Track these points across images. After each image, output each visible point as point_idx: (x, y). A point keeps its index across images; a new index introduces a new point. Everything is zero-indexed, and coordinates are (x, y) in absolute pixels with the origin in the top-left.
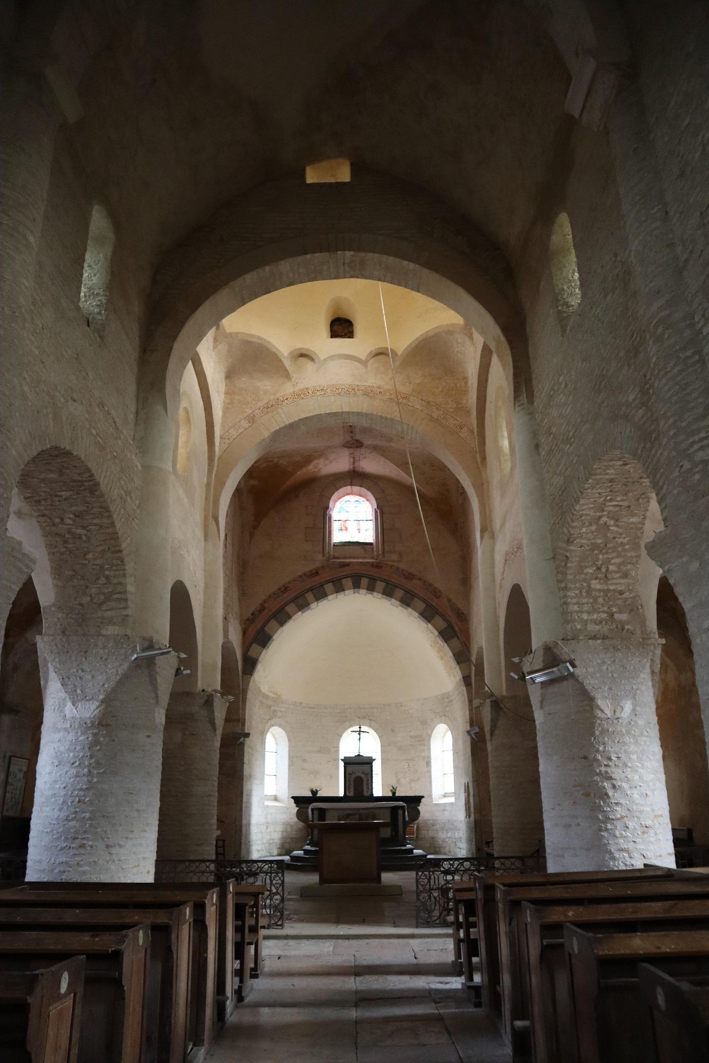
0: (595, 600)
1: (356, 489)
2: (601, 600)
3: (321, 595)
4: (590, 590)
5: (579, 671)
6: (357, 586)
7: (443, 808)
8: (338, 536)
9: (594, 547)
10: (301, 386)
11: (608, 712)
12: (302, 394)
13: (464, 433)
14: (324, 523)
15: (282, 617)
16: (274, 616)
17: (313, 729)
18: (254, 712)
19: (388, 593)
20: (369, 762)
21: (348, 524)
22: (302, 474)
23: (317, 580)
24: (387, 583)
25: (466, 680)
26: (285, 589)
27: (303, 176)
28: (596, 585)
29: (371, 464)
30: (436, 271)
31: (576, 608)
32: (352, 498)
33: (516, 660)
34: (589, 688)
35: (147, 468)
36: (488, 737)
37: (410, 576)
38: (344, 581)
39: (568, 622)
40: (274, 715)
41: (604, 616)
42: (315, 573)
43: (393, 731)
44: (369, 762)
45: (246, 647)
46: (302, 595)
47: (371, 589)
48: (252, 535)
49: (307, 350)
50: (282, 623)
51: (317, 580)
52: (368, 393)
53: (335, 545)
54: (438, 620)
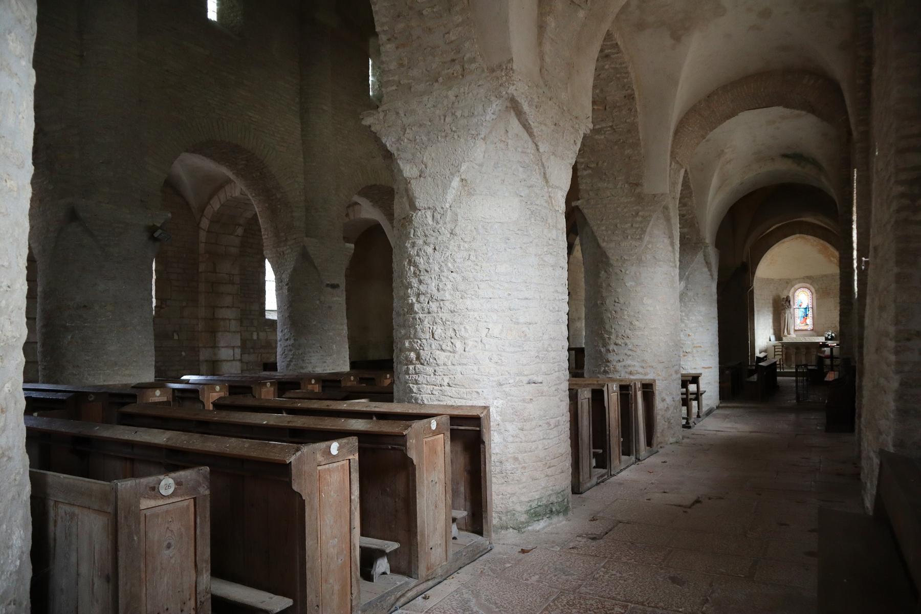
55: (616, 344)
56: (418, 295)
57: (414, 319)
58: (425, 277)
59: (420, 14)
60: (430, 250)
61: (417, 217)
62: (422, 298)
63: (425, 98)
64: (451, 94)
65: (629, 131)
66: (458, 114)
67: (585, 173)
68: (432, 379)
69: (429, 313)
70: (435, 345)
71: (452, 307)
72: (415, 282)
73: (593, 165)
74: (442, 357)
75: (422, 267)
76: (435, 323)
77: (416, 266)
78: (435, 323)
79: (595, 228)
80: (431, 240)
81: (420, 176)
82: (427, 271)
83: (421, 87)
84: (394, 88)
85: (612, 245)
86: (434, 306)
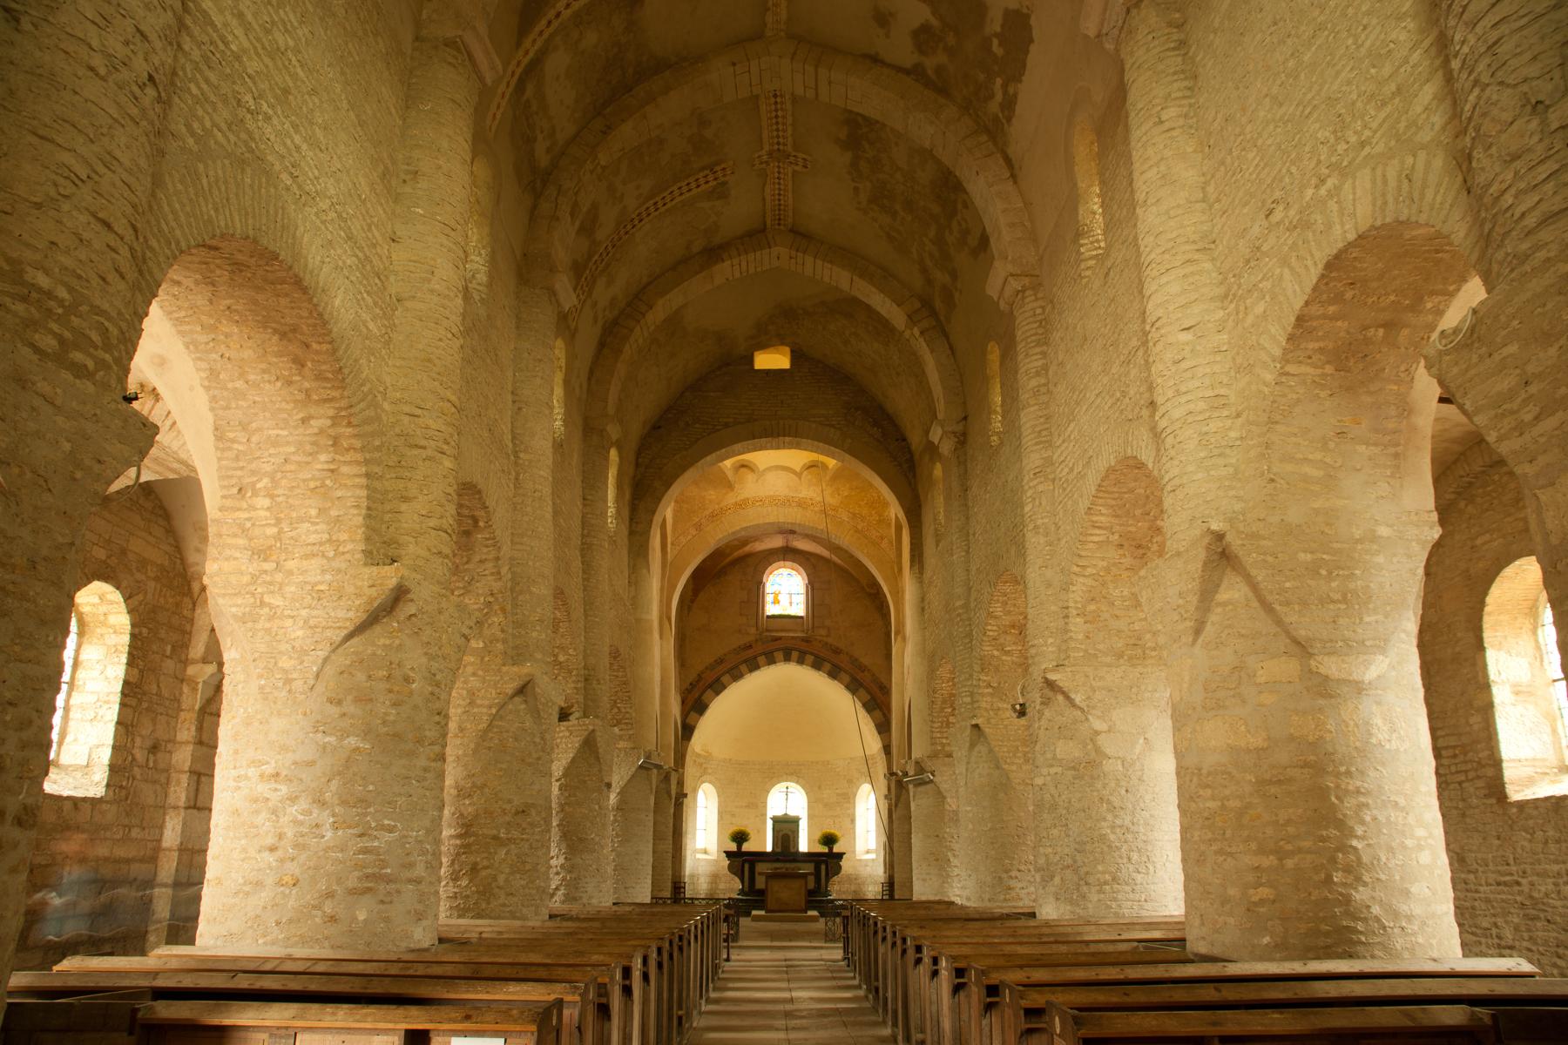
3: (754, 667)
5: (937, 779)
6: (787, 659)
7: (866, 863)
10: (742, 497)
13: (884, 544)
15: (718, 687)
16: (710, 686)
17: (746, 784)
18: (690, 770)
19: (817, 666)
20: (795, 821)
22: (736, 554)
23: (750, 653)
24: (816, 656)
25: (887, 749)
26: (720, 661)
27: (751, 361)
32: (781, 571)
35: (638, 621)
37: (837, 651)
40: (705, 772)
44: (795, 821)
45: (685, 715)
46: (736, 667)
47: (801, 662)
48: (689, 608)
50: (718, 693)
51: (750, 653)
52: (802, 504)
54: (862, 691)
56: (1113, 827)
57: (1110, 847)
61: (1108, 766)
70: (1131, 868)
72: (1110, 817)
74: (1139, 878)
83: (1108, 659)
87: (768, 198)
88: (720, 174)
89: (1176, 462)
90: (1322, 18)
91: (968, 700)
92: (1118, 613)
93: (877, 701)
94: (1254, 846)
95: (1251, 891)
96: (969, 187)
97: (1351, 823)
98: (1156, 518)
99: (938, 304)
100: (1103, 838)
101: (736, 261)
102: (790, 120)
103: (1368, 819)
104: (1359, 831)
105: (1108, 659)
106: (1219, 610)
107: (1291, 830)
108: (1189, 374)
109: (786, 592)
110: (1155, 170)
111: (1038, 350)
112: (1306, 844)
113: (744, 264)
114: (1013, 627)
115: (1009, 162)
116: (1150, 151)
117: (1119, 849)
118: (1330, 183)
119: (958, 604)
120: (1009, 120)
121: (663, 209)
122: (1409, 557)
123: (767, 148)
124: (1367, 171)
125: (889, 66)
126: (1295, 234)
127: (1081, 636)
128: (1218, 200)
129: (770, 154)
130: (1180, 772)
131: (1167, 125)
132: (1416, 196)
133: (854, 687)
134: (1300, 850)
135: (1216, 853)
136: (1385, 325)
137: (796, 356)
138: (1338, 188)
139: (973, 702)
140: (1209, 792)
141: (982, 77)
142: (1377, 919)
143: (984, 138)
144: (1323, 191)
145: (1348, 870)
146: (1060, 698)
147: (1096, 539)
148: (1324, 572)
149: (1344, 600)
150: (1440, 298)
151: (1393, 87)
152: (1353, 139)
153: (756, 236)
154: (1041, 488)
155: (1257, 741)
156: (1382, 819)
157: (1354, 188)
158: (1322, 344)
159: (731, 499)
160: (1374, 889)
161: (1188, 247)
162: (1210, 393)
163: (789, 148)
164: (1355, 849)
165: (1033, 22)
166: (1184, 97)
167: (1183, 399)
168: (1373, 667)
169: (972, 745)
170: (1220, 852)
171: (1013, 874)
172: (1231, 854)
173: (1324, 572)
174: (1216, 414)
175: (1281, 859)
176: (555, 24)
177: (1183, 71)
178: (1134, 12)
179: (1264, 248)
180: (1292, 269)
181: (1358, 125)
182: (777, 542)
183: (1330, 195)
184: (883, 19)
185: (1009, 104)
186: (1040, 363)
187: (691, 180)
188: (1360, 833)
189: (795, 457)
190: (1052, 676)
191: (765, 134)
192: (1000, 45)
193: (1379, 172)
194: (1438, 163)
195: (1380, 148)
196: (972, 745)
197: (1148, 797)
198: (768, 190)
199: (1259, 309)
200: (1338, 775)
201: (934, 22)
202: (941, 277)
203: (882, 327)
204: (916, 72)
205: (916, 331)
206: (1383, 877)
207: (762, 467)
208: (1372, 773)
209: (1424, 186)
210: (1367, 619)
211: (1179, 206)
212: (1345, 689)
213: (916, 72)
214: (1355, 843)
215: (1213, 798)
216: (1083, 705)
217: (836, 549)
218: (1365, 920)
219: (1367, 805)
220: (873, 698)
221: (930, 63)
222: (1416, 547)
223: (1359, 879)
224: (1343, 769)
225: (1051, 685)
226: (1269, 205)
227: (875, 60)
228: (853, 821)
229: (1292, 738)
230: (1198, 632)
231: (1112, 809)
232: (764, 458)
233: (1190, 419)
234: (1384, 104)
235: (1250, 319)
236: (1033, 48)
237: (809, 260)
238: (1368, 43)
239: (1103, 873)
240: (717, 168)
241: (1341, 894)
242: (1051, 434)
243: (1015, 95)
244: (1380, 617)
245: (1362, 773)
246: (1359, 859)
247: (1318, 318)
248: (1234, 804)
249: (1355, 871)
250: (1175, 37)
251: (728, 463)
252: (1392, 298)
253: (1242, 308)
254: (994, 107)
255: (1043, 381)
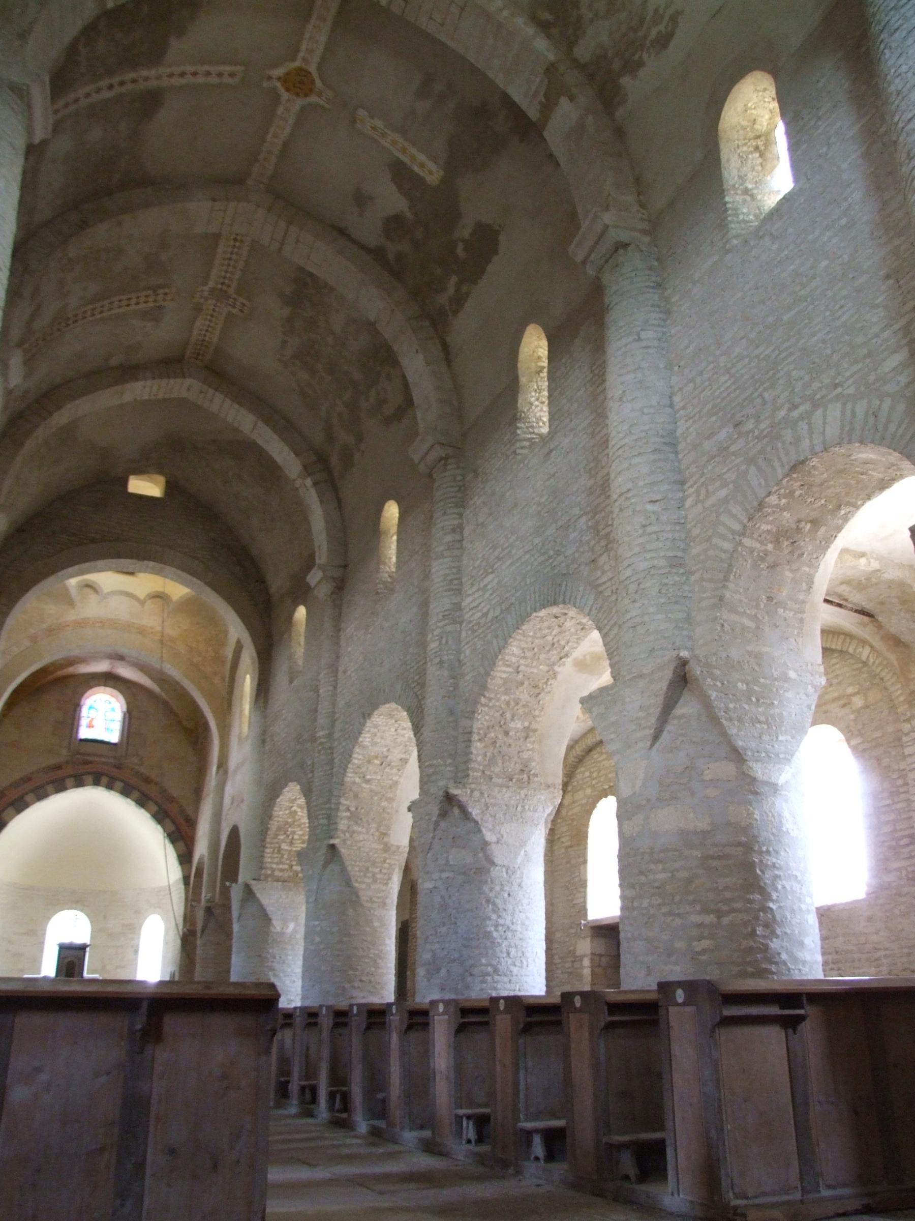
0: (282, 856)
1: (109, 690)
2: (286, 856)
4: (279, 849)
6: (96, 783)
8: (84, 733)
9: (287, 823)
11: (278, 929)
12: (81, 624)
14: (73, 724)
21: (94, 723)
25: (186, 879)
26: (28, 779)
28: (284, 846)
29: (126, 672)
30: (216, 590)
31: (269, 860)
33: (228, 884)
34: (269, 913)
36: (199, 934)
37: (147, 780)
38: (84, 777)
39: (262, 868)
41: (286, 867)
42: (58, 767)
43: (105, 917)
46: (42, 786)
49: (93, 582)
50: (19, 811)
51: (60, 774)
52: (142, 631)
53: (82, 740)
54: (168, 822)
55: (361, 981)
57: (493, 942)
58: (504, 914)
59: (506, 733)
60: (506, 895)
61: (495, 872)
62: (500, 928)
63: (505, 790)
64: (523, 792)
65: (390, 787)
66: (527, 807)
67: (345, 814)
68: (508, 986)
69: (506, 939)
70: (510, 961)
71: (521, 936)
72: (494, 917)
73: (353, 809)
74: (515, 970)
75: (500, 906)
76: (510, 946)
77: (494, 904)
78: (510, 946)
79: (349, 868)
80: (506, 888)
81: (498, 842)
82: (505, 910)
83: (500, 781)
84: (479, 774)
85: (364, 886)
86: (509, 934)
87: (195, 332)
88: (160, 298)
89: (638, 604)
90: (802, 292)
91: (324, 821)
92: (511, 741)
93: (181, 835)
94: (698, 908)
95: (695, 943)
96: (405, 362)
97: (769, 890)
98: (554, 664)
99: (335, 461)
100: (488, 935)
101: (149, 383)
102: (241, 264)
103: (780, 887)
104: (774, 896)
105: (500, 781)
106: (675, 722)
107: (728, 895)
108: (654, 536)
109: (102, 717)
110: (633, 376)
111: (456, 510)
112: (738, 905)
113: (155, 388)
114: (376, 757)
115: (445, 347)
116: (629, 360)
117: (500, 945)
118: (802, 409)
119: (321, 733)
120: (456, 312)
121: (99, 316)
122: (807, 695)
123: (211, 284)
124: (839, 406)
125: (353, 241)
126: (765, 441)
127: (479, 758)
128: (684, 408)
129: (212, 291)
130: (623, 857)
131: (644, 343)
132: (880, 427)
133: (160, 817)
134: (734, 910)
135: (664, 915)
136: (812, 522)
137: (171, 487)
138: (809, 415)
139: (329, 825)
140: (660, 867)
141: (439, 271)
142: (785, 964)
143: (427, 323)
144: (795, 414)
145: (766, 926)
146: (456, 811)
147: (504, 676)
148: (754, 699)
149: (766, 722)
150: (851, 509)
151: (865, 351)
152: (827, 381)
153: (171, 364)
154: (449, 628)
155: (703, 824)
156: (788, 888)
157: (825, 417)
158: (769, 527)
159: (71, 616)
160: (783, 939)
161: (658, 440)
162: (670, 554)
163: (231, 291)
164: (771, 909)
165: (502, 238)
166: (659, 326)
167: (648, 556)
168: (783, 775)
169: (326, 865)
170: (670, 913)
171: (356, 984)
172: (679, 915)
173: (754, 699)
174: (674, 571)
175: (719, 918)
176: (72, 108)
177: (659, 306)
178: (621, 251)
179: (733, 448)
180: (759, 468)
181: (832, 372)
182: (102, 667)
183: (801, 418)
184: (361, 200)
185: (459, 301)
186: (456, 522)
187: (134, 295)
188: (774, 898)
189: (146, 582)
190: (454, 791)
191: (215, 272)
192: (465, 249)
193: (849, 406)
194: (901, 407)
195: (852, 390)
196: (326, 865)
197: (525, 901)
198: (198, 324)
199: (723, 493)
200: (761, 852)
201: (409, 215)
202: (344, 437)
203: (270, 472)
204: (378, 254)
205: (309, 482)
206: (789, 932)
207: (106, 591)
208: (782, 853)
209: (889, 421)
210: (781, 738)
211: (651, 406)
212: (767, 789)
213: (378, 254)
214: (771, 905)
215: (664, 870)
216: (478, 818)
217: (161, 678)
218: (776, 963)
219: (779, 877)
220: (178, 829)
221: (392, 249)
222: (810, 689)
223: (773, 932)
224: (764, 849)
225: (449, 799)
226: (738, 417)
227: (343, 232)
228: (136, 952)
229: (729, 824)
230: (656, 738)
231: (496, 910)
232: (107, 579)
233: (653, 572)
234: (856, 362)
235: (709, 503)
236: (496, 259)
237: (219, 397)
238: (844, 318)
239: (487, 965)
240: (161, 291)
241: (763, 944)
242: (461, 584)
243: (467, 295)
244: (789, 738)
245: (777, 852)
246: (774, 916)
247: (773, 506)
248: (685, 874)
249: (771, 925)
250: (653, 279)
251: (73, 582)
252: (823, 502)
253: (703, 492)
254: (443, 299)
255: (458, 537)
